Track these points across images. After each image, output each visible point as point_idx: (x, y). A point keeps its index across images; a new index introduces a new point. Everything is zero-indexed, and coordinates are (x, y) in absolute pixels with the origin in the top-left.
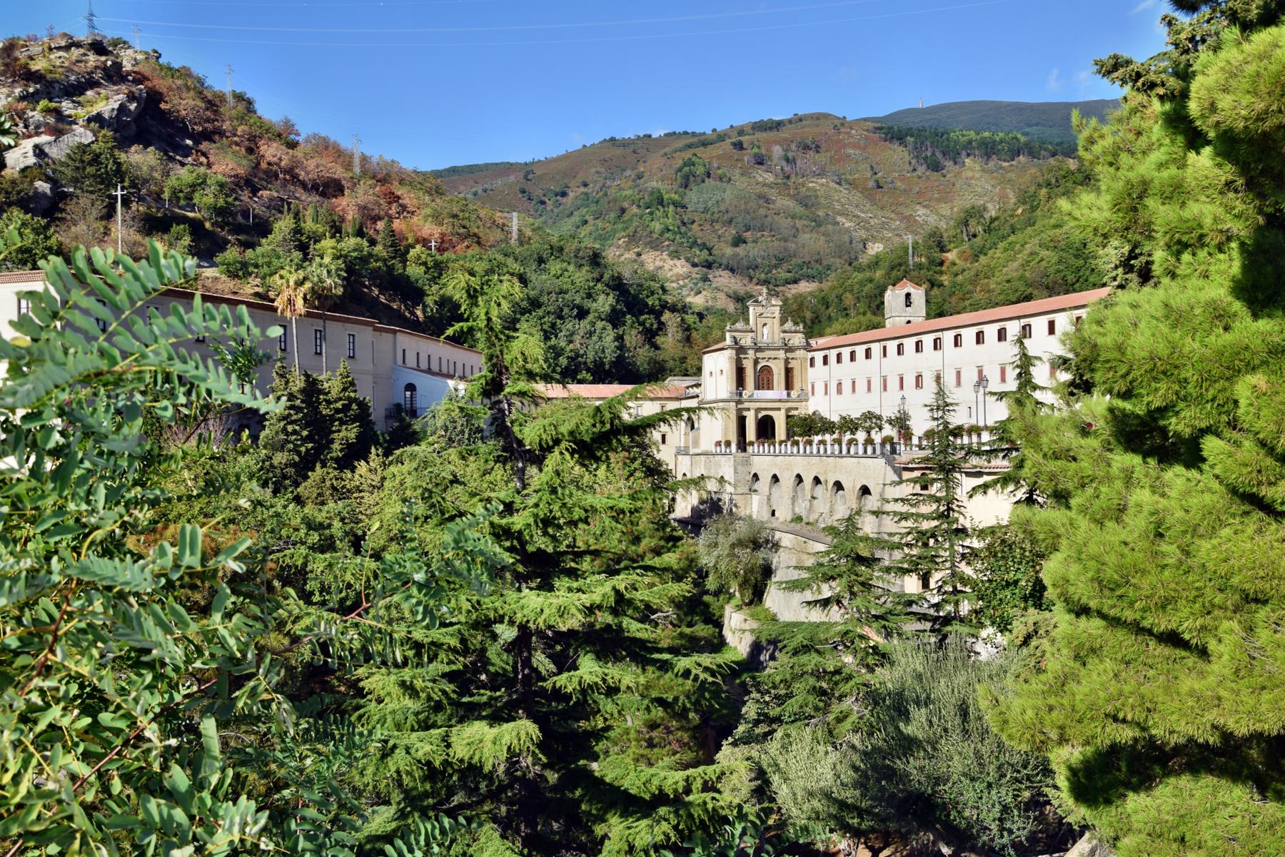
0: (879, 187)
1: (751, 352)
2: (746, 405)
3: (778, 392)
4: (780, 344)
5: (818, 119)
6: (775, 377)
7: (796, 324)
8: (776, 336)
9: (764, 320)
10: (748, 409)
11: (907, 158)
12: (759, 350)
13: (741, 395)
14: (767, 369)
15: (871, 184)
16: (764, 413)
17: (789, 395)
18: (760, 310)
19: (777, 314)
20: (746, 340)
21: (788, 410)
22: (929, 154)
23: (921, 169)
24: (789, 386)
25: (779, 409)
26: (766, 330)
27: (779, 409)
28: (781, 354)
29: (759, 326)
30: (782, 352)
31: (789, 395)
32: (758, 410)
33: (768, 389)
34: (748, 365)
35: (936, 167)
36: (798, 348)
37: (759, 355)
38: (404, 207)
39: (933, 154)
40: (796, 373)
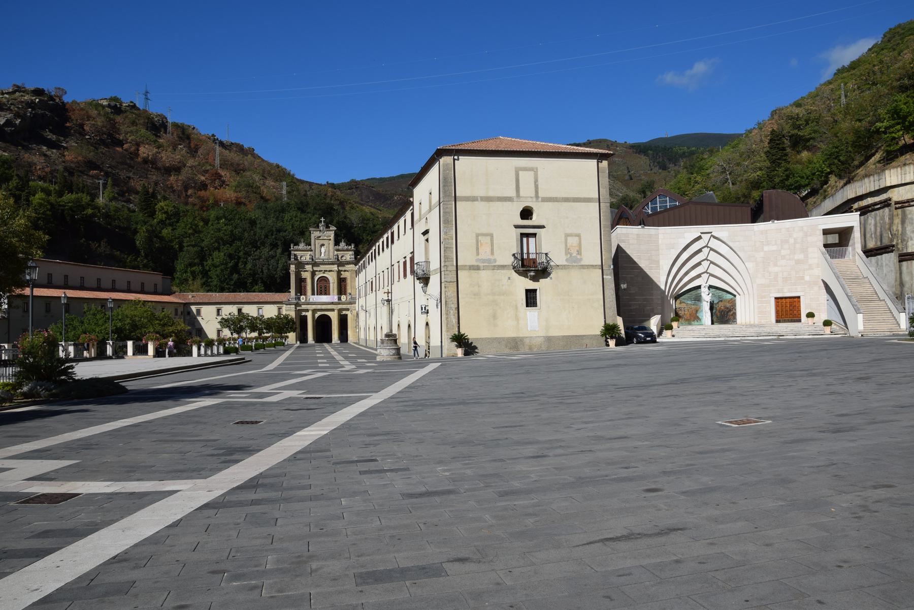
0: (631, 179)
2: (304, 307)
3: (333, 297)
4: (333, 259)
5: (600, 142)
6: (331, 285)
7: (348, 244)
8: (331, 254)
9: (322, 242)
10: (307, 310)
11: (648, 162)
12: (315, 264)
13: (299, 299)
14: (324, 280)
15: (627, 177)
18: (317, 234)
20: (306, 257)
21: (340, 310)
22: (661, 160)
23: (656, 169)
24: (342, 290)
25: (333, 310)
26: (323, 250)
28: (335, 268)
31: (339, 299)
32: (314, 311)
34: (306, 275)
35: (664, 168)
36: (349, 263)
37: (315, 269)
38: (224, 182)
39: (663, 160)
40: (348, 281)
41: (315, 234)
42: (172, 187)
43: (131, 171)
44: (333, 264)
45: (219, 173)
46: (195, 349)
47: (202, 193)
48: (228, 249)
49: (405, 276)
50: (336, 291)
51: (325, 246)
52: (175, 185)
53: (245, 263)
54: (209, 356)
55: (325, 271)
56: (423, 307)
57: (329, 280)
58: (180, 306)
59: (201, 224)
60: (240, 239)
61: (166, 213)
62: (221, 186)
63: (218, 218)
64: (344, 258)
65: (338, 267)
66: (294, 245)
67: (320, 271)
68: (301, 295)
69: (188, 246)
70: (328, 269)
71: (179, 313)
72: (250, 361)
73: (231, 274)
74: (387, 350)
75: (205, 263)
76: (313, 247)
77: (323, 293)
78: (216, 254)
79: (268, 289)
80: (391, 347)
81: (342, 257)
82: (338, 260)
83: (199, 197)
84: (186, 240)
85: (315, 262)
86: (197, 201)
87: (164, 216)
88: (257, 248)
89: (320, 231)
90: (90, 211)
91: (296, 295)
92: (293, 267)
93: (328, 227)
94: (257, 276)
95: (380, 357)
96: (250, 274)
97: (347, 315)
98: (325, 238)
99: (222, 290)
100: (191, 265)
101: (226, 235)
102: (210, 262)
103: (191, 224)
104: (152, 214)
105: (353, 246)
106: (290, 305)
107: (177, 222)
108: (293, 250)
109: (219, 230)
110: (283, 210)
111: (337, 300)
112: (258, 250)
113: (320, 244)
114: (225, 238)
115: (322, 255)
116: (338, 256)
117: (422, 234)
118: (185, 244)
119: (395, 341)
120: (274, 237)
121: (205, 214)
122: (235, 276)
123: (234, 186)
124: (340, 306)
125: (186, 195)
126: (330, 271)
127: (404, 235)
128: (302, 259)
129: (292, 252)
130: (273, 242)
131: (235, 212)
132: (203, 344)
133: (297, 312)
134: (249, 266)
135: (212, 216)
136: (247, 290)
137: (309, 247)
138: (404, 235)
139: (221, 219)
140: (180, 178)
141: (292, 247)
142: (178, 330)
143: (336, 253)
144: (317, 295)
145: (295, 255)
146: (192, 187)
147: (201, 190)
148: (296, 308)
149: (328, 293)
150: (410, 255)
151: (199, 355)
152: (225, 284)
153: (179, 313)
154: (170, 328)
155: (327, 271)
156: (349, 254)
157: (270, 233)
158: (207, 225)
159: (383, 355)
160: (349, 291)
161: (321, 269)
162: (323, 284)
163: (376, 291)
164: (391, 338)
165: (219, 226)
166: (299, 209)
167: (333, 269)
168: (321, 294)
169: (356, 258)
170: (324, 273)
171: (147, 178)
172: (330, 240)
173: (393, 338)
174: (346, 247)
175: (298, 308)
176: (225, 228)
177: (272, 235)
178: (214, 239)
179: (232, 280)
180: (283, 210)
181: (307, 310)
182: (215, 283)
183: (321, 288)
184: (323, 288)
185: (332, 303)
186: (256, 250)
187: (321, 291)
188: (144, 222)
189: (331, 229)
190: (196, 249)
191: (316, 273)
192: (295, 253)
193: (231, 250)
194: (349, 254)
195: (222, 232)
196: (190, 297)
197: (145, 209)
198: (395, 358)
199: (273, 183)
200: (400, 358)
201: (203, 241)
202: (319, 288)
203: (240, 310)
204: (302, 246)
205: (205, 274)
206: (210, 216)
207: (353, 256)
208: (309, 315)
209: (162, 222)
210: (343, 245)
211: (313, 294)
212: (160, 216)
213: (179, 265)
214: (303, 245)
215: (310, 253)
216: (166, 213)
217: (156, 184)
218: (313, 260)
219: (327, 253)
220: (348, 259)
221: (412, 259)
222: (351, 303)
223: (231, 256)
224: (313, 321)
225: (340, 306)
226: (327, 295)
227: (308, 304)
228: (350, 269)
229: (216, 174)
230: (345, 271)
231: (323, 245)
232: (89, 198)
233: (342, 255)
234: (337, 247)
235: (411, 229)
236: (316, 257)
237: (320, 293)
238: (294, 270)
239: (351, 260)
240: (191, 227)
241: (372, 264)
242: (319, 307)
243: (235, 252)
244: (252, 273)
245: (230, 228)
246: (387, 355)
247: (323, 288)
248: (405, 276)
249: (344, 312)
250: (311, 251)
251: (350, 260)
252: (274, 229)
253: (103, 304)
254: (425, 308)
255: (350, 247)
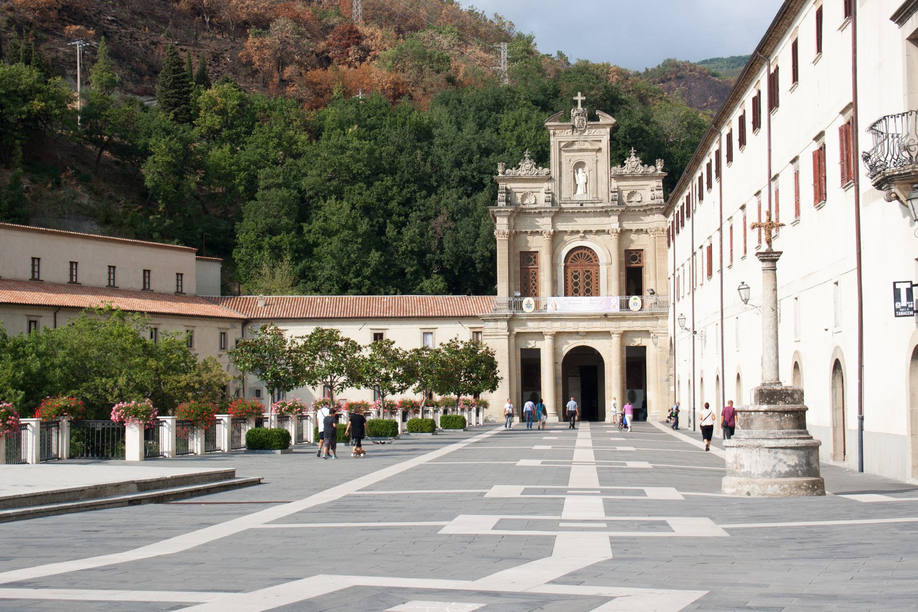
1: (545, 224)
2: (532, 326)
6: (603, 270)
7: (648, 161)
9: (578, 157)
10: (540, 335)
12: (558, 213)
13: (519, 306)
16: (573, 343)
17: (625, 305)
19: (605, 144)
25: (607, 334)
26: (581, 177)
27: (607, 334)
28: (612, 223)
29: (567, 168)
30: (614, 219)
31: (625, 305)
32: (557, 336)
33: (588, 293)
34: (539, 244)
36: (647, 210)
38: (367, 51)
41: (558, 136)
42: (250, 63)
43: (162, 32)
44: (606, 213)
45: (357, 31)
46: (133, 436)
47: (318, 74)
48: (360, 194)
49: (820, 195)
50: (614, 285)
51: (586, 168)
52: (255, 58)
53: (400, 226)
54: (197, 458)
55: (585, 232)
56: (903, 288)
57: (596, 257)
58: (234, 327)
59: (304, 137)
60: (393, 172)
61: (222, 112)
62: (362, 60)
63: (343, 125)
64: (636, 198)
65: (620, 221)
66: (506, 168)
67: (573, 233)
68: (525, 294)
69: (267, 188)
70: (594, 229)
71: (231, 343)
72: (257, 482)
73: (365, 250)
74: (765, 452)
75: (306, 227)
76: (554, 170)
77: (581, 291)
78: (331, 205)
79: (455, 287)
80: (783, 443)
81: (632, 194)
82: (620, 202)
83: (311, 84)
84: (262, 173)
85: (561, 208)
86: (306, 93)
87: (217, 119)
88: (431, 190)
89: (573, 127)
90: (37, 105)
91: (510, 294)
92: (502, 225)
93: (593, 118)
94: (429, 256)
95: (733, 479)
96: (412, 251)
97: (644, 348)
98: (587, 146)
99: (344, 289)
100: (272, 231)
101: (360, 160)
102: (317, 224)
103: (280, 138)
104: (188, 116)
105: (659, 167)
106: (496, 320)
107: (249, 133)
108: (503, 180)
109: (343, 149)
110: (498, 106)
111: (618, 307)
112: (433, 196)
113: (573, 163)
114: (355, 168)
115: (580, 190)
116: (619, 191)
117: (893, 18)
118: (262, 184)
119: (799, 417)
120: (473, 166)
121: (312, 116)
122: (375, 256)
123: (389, 59)
124: (626, 326)
125: (282, 81)
126: (598, 232)
127: (815, 62)
128: (526, 202)
129: (502, 185)
130: (473, 177)
131: (384, 110)
132: (225, 418)
133: (513, 340)
134: (409, 233)
135: (329, 119)
136: (406, 290)
137: (546, 170)
138: (815, 62)
139: (350, 123)
140: (268, 41)
141: (500, 170)
142: (201, 383)
143: (615, 184)
144: (566, 295)
145: (508, 192)
146: (292, 61)
147: (314, 68)
148: (510, 330)
149: (593, 290)
150: (842, 121)
151: (151, 453)
152: (351, 275)
153: (231, 343)
154: (183, 376)
155: (591, 231)
156: (648, 188)
157: (466, 157)
158: (317, 139)
159: (747, 474)
160: (649, 283)
161: (575, 228)
162: (580, 267)
163: (721, 271)
164: (780, 406)
165: (342, 141)
166: (536, 103)
167: (606, 228)
168: (576, 293)
169: (666, 198)
170: (583, 238)
171: (196, 45)
172: (600, 150)
173: (789, 407)
174: (641, 169)
175: (517, 330)
176: (356, 143)
177: (470, 161)
178: (330, 170)
179: (366, 264)
180: (498, 106)
181: (540, 335)
182: (326, 273)
183: (576, 277)
184: (581, 278)
185: (606, 315)
186: (429, 195)
187: (576, 284)
188: (164, 130)
189: (601, 121)
190: (284, 192)
191: (566, 238)
192: (509, 186)
193: (370, 197)
194: (648, 188)
195: (349, 153)
196: (261, 304)
197: (176, 105)
198: (799, 487)
199: (483, 54)
200: (817, 487)
201: (305, 175)
202: (570, 277)
203: (378, 337)
204: (526, 167)
205: (304, 251)
206: (324, 118)
207: (660, 193)
208: (545, 348)
209: (213, 135)
210: (633, 162)
211: (554, 294)
212: (209, 120)
213: (246, 233)
214: (529, 166)
215: (546, 185)
216: (222, 112)
217: (216, 57)
218: (553, 202)
219: (591, 185)
220: (647, 200)
221: (849, 133)
222: (654, 317)
223: (367, 210)
224: (555, 363)
225: (626, 326)
226: (591, 295)
227: (543, 319)
228: (655, 225)
229: (350, 32)
230: (639, 231)
231: (580, 165)
232: (36, 74)
233: (632, 189)
234: (617, 169)
235: (842, 28)
236: (563, 196)
237: (573, 289)
238: (507, 231)
239: (655, 202)
240: (279, 144)
241: (711, 196)
242: (570, 326)
243: (379, 200)
244: (416, 249)
245: (367, 145)
246: (765, 474)
247: (581, 278)
248: (820, 195)
249: (638, 342)
250: (549, 179)
251: (652, 202)
252: (474, 147)
253: (33, 319)
254: (910, 292)
255: (651, 169)
